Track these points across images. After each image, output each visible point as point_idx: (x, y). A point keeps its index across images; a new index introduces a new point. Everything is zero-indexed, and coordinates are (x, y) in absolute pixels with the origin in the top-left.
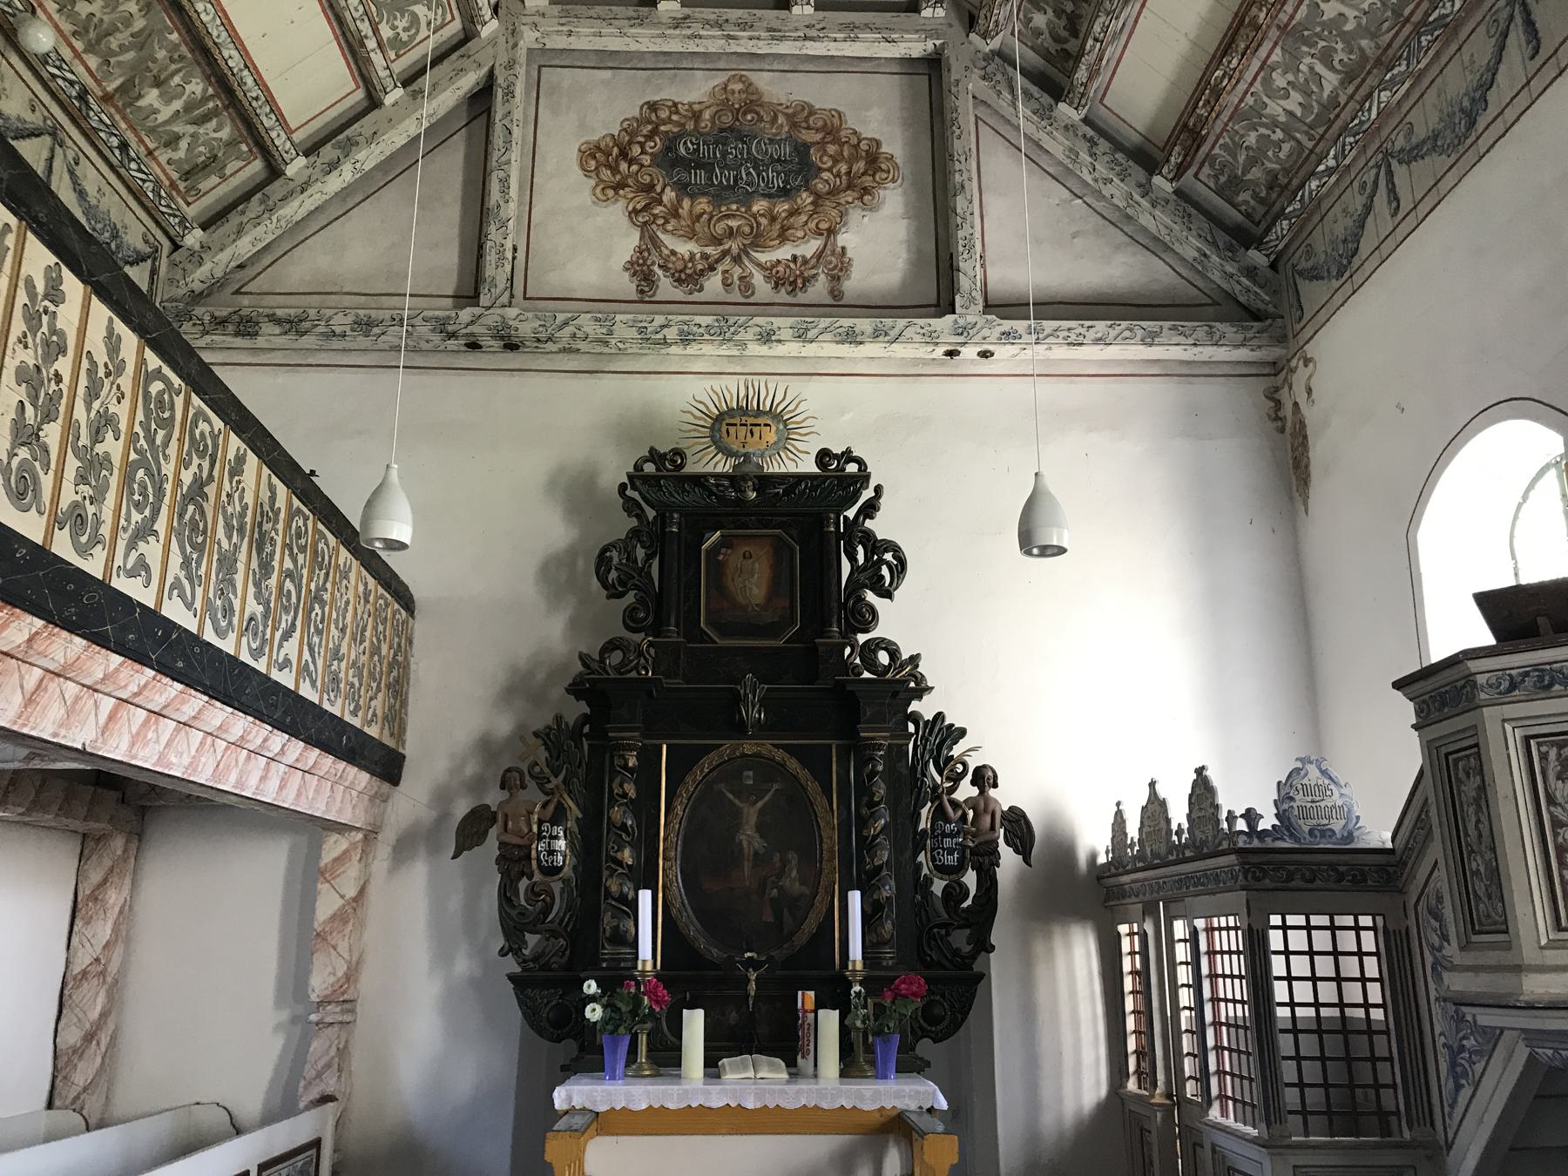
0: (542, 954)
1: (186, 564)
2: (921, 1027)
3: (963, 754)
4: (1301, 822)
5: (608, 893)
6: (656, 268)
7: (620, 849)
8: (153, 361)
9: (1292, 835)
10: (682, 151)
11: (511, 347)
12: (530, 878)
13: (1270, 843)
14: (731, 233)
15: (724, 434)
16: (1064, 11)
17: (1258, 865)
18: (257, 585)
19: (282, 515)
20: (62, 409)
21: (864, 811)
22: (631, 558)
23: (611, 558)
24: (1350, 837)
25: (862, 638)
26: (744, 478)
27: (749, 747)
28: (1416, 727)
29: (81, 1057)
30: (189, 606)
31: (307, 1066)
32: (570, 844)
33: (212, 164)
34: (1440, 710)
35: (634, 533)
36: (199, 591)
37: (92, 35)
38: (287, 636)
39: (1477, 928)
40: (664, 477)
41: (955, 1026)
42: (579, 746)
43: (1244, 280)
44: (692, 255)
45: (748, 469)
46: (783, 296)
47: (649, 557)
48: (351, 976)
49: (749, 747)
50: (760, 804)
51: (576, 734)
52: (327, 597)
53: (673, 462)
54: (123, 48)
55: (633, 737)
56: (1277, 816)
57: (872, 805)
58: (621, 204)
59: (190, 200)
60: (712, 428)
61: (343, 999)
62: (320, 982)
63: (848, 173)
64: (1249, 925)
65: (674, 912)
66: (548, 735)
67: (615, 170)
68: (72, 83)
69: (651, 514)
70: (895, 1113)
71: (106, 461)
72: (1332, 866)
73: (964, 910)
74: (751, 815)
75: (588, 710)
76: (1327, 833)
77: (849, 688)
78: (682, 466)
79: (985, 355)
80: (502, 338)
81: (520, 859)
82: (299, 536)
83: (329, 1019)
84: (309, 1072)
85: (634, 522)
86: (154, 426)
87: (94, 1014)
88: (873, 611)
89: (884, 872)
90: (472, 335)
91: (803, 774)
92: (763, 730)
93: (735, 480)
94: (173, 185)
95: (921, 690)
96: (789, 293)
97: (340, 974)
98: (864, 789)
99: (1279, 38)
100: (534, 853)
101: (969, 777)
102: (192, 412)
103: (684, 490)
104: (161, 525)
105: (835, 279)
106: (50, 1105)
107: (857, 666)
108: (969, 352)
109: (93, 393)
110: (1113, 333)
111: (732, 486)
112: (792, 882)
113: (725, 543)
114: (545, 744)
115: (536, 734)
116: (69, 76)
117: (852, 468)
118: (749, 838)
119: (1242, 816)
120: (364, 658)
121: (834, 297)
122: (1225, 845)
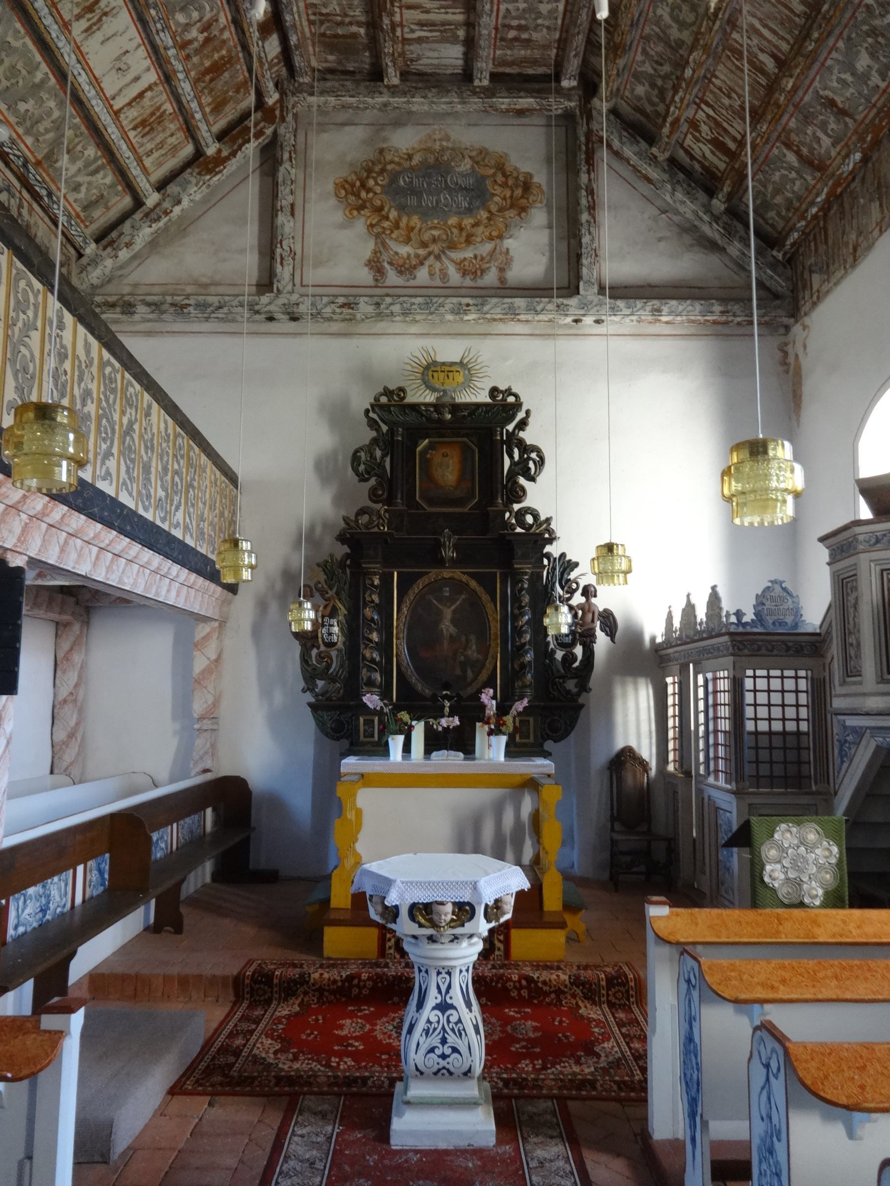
0: (327, 692)
1: (128, 471)
2: (547, 734)
3: (577, 578)
4: (768, 618)
5: (364, 656)
6: (386, 264)
7: (371, 633)
8: (106, 355)
9: (762, 625)
10: (402, 183)
11: (294, 319)
12: (318, 648)
13: (749, 629)
14: (434, 240)
15: (431, 378)
16: (656, 85)
17: (741, 642)
18: (162, 480)
19: (171, 437)
20: (68, 390)
21: (516, 611)
22: (373, 457)
23: (360, 457)
24: (796, 626)
25: (516, 507)
26: (443, 406)
27: (446, 574)
28: (829, 564)
29: (67, 746)
30: (131, 494)
31: (194, 753)
32: (341, 630)
33: (101, 199)
35: (375, 441)
36: (135, 485)
37: (28, 123)
38: (177, 509)
40: (393, 406)
41: (566, 734)
42: (344, 572)
43: (769, 272)
44: (409, 256)
45: (447, 399)
46: (468, 282)
47: (383, 457)
48: (216, 704)
49: (446, 574)
50: (453, 607)
51: (342, 565)
52: (196, 484)
53: (399, 395)
54: (47, 131)
55: (376, 567)
56: (755, 614)
57: (521, 607)
58: (363, 220)
59: (87, 224)
60: (423, 374)
61: (211, 715)
62: (198, 707)
63: (511, 197)
65: (403, 669)
66: (326, 566)
67: (358, 196)
68: (18, 157)
69: (385, 428)
70: (529, 777)
71: (88, 417)
72: (784, 642)
74: (448, 613)
75: (349, 551)
76: (782, 624)
77: (508, 538)
78: (404, 398)
79: (598, 322)
80: (288, 313)
81: (312, 638)
82: (180, 449)
83: (205, 727)
84: (196, 756)
85: (374, 434)
86: (108, 393)
87: (73, 723)
88: (523, 490)
89: (527, 647)
90: (270, 312)
91: (479, 590)
92: (456, 563)
93: (437, 407)
94: (78, 216)
95: (551, 541)
96: (472, 280)
97: (210, 702)
98: (516, 599)
99: (794, 112)
100: (320, 635)
101: (580, 591)
102: (125, 382)
103: (405, 413)
104: (115, 450)
105: (502, 270)
106: (52, 772)
107: (513, 524)
108: (588, 320)
109: (81, 379)
110: (681, 308)
111: (436, 411)
112: (473, 652)
113: (431, 446)
114: (324, 570)
115: (318, 565)
116: (17, 152)
117: (511, 399)
118: (447, 627)
119: (734, 614)
120: (216, 520)
121: (502, 282)
122: (724, 630)
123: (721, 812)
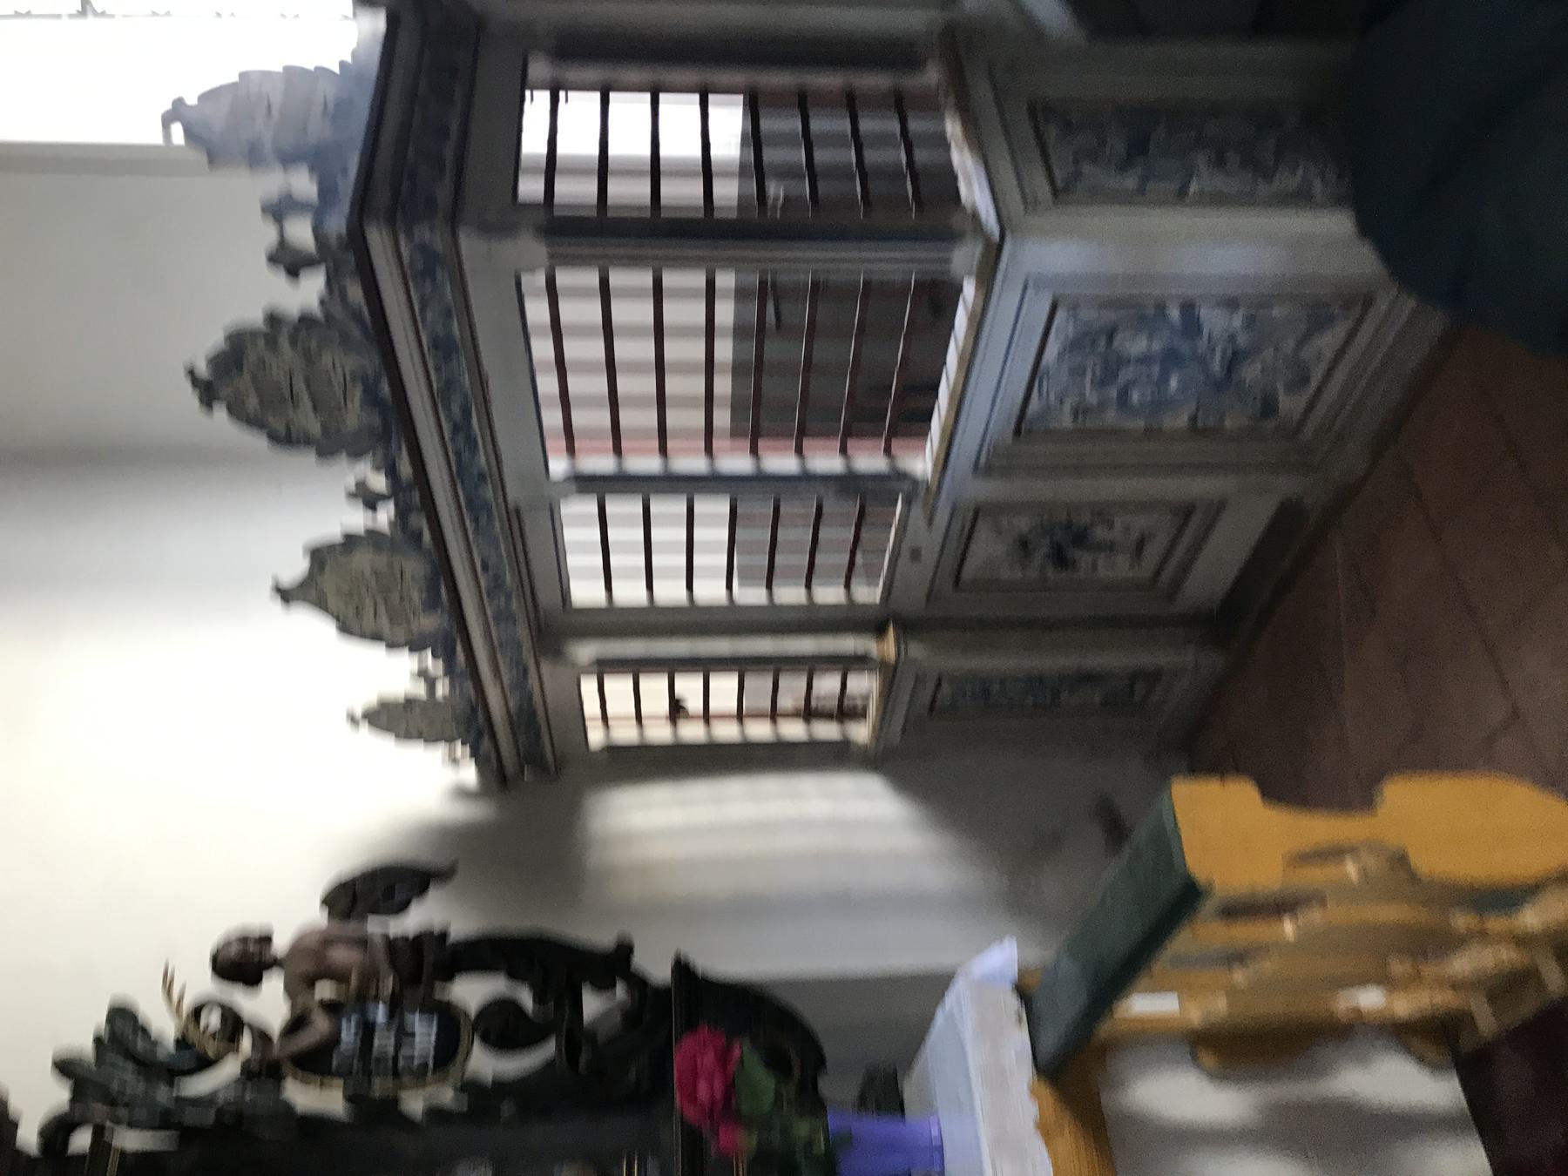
73: (539, 999)
122: (355, 293)
123: (1035, 404)
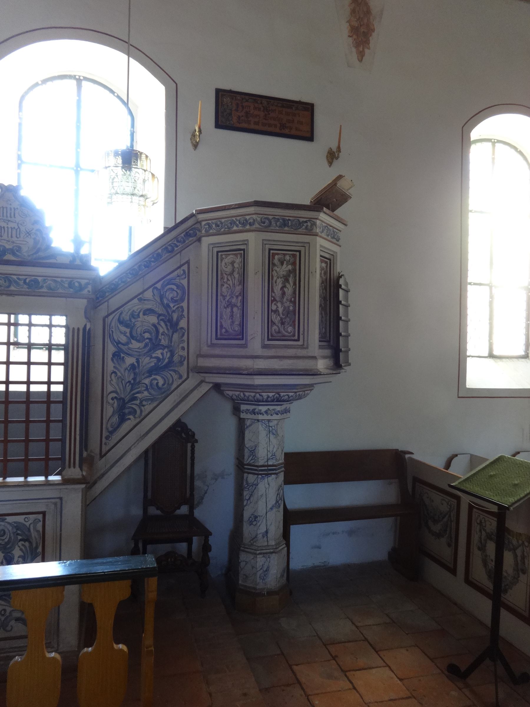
34: (280, 227)
39: (270, 337)
64: (85, 326)
